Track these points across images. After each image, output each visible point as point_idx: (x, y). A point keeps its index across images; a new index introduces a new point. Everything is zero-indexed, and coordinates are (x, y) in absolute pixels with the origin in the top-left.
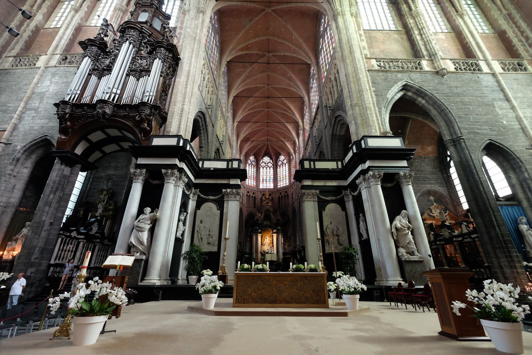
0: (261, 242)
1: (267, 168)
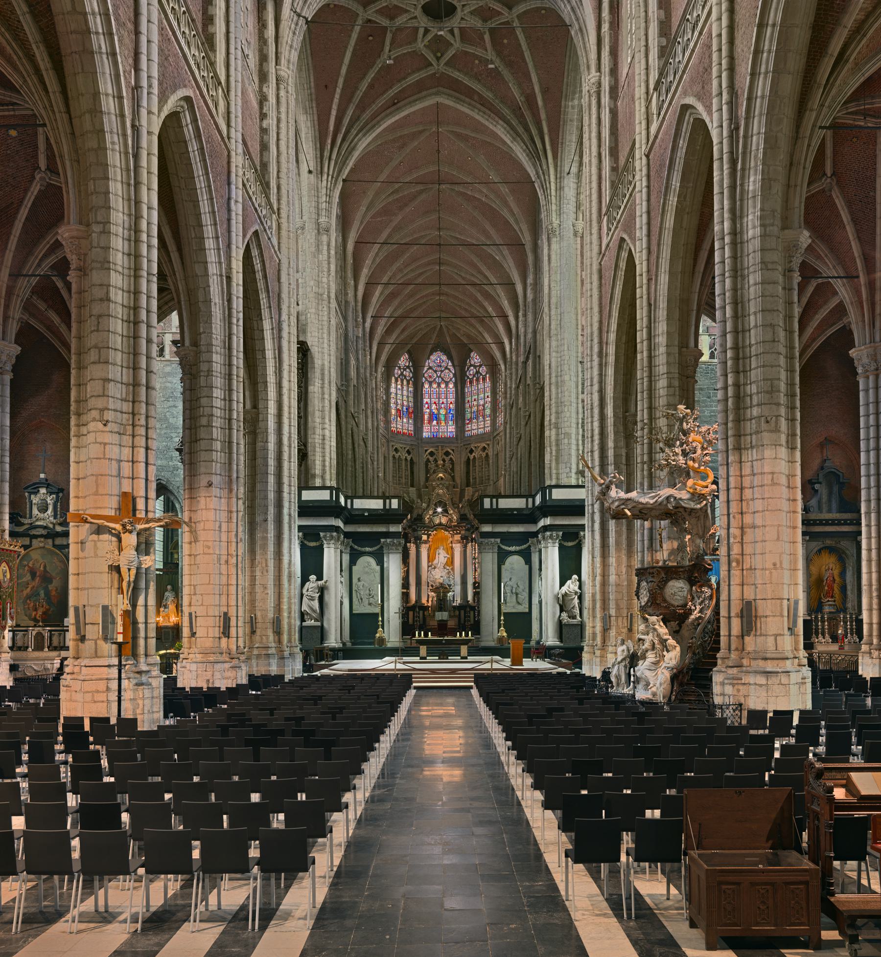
0: (429, 562)
1: (439, 385)
